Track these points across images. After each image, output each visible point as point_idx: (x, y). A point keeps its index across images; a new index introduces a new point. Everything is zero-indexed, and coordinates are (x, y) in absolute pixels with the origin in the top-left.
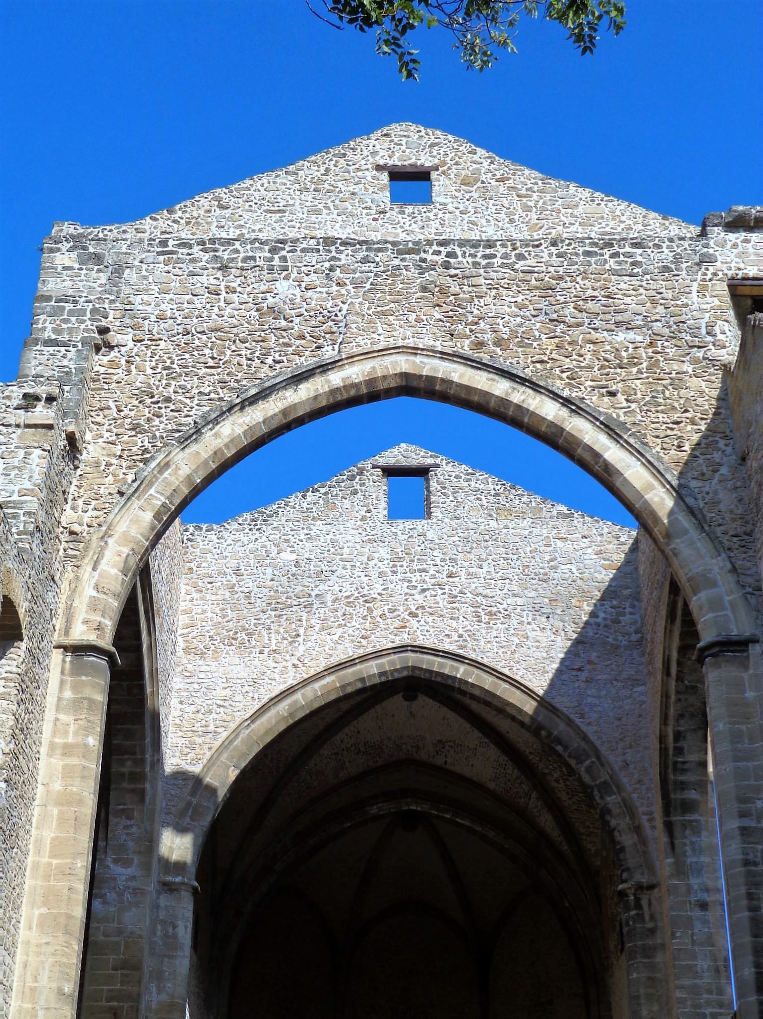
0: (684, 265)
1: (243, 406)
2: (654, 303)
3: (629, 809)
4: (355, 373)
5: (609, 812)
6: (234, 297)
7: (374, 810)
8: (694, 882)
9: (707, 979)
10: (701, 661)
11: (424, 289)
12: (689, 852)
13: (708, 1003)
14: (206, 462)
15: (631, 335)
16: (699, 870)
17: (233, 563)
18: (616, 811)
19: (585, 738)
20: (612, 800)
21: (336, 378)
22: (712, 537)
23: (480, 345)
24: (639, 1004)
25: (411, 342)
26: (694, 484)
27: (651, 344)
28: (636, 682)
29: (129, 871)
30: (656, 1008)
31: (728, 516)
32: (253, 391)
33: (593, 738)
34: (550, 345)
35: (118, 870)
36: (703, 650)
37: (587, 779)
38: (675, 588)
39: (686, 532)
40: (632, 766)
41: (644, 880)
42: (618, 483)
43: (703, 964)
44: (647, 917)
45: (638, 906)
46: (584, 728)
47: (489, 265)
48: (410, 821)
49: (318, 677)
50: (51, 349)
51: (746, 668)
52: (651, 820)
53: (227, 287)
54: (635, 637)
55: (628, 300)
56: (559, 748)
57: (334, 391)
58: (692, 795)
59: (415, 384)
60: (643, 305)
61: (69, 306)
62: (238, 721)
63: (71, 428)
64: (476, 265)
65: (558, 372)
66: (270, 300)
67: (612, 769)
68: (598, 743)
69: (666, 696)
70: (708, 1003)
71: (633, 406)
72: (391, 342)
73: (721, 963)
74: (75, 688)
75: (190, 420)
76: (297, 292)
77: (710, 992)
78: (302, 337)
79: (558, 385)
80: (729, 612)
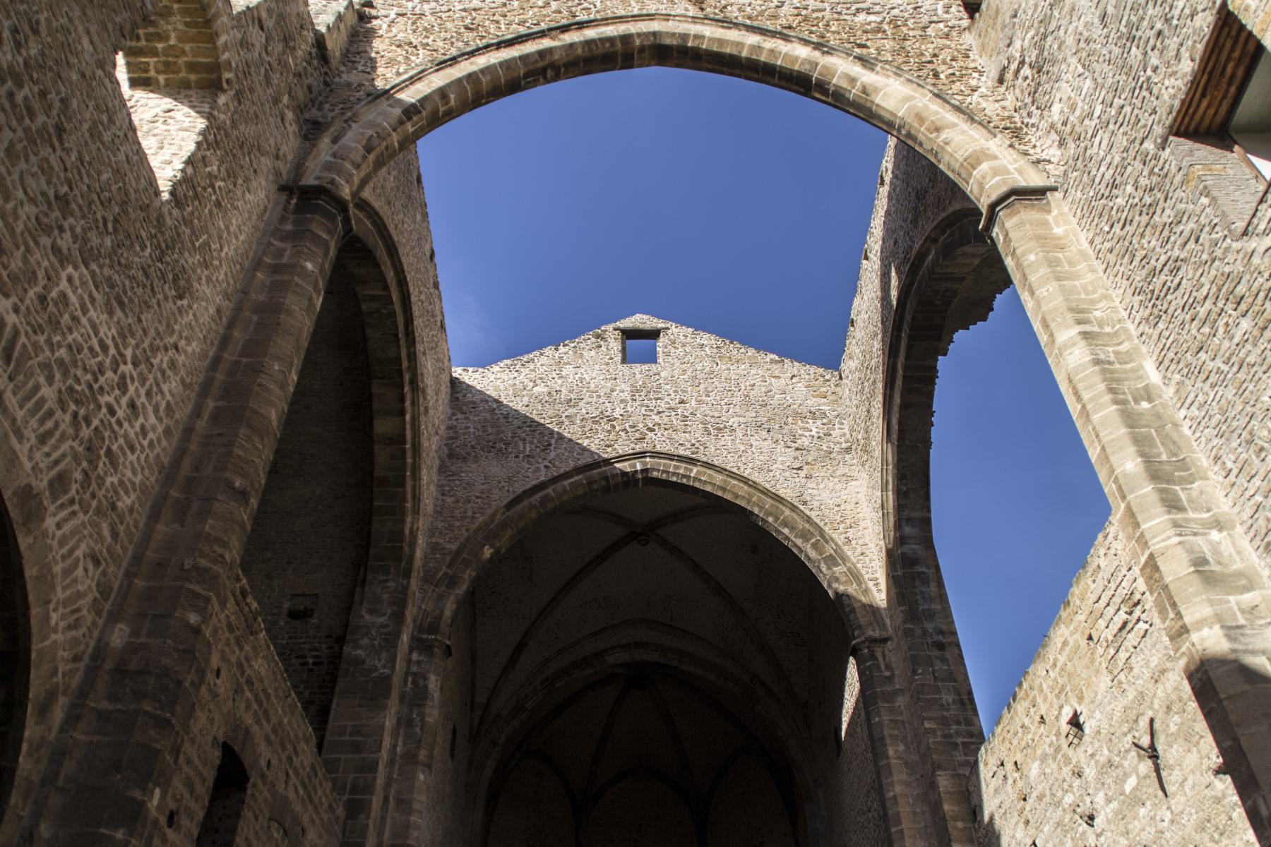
5: (837, 580)
8: (929, 626)
9: (953, 711)
12: (921, 601)
13: (958, 733)
15: (872, 18)
16: (931, 615)
19: (809, 520)
24: (885, 745)
31: (995, 118)
33: (817, 520)
39: (955, 125)
40: (853, 542)
41: (877, 634)
43: (947, 698)
44: (882, 666)
46: (808, 513)
51: (1049, 212)
54: (844, 445)
56: (786, 531)
67: (836, 544)
68: (821, 524)
70: (958, 733)
73: (965, 697)
74: (295, 223)
77: (959, 723)
80: (1016, 175)
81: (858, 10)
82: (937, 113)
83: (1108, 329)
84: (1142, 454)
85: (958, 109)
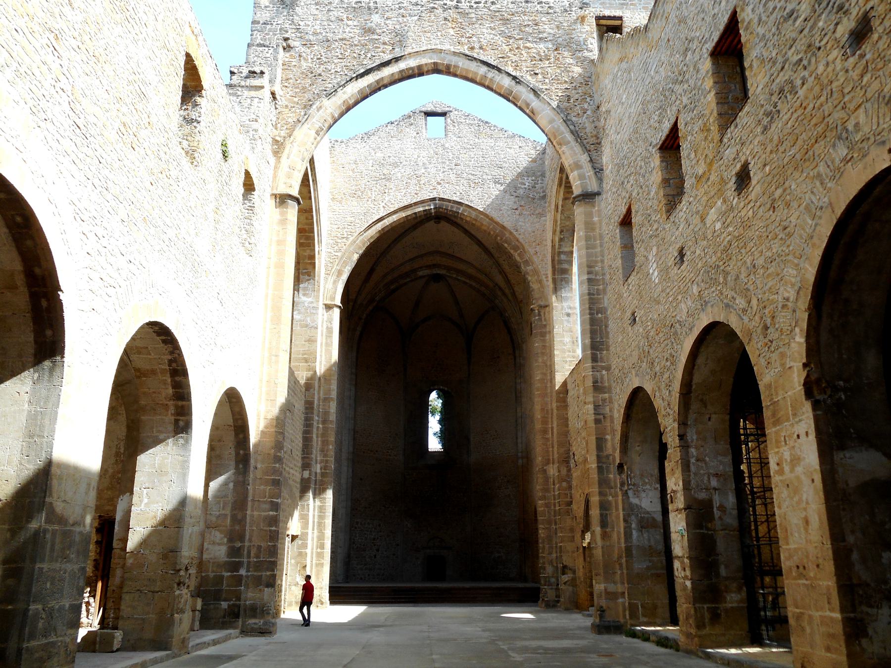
0: (574, 9)
1: (357, 78)
2: (558, 27)
3: (536, 272)
4: (412, 63)
5: (528, 273)
6: (350, 23)
7: (421, 273)
8: (565, 304)
9: (569, 346)
10: (573, 203)
11: (445, 19)
13: (568, 356)
14: (340, 107)
16: (567, 299)
17: (354, 158)
18: (531, 273)
20: (529, 268)
21: (402, 65)
22: (582, 145)
23: (472, 48)
25: (439, 47)
26: (574, 119)
27: (556, 50)
28: (541, 215)
29: (310, 299)
30: (545, 358)
31: (589, 135)
32: (362, 71)
33: (521, 240)
34: (507, 49)
35: (304, 299)
36: (574, 198)
37: (518, 259)
38: (562, 170)
39: (569, 142)
42: (538, 119)
45: (539, 315)
46: (517, 236)
47: (477, 8)
48: (437, 278)
49: (395, 212)
50: (261, 49)
51: (594, 206)
52: (547, 277)
53: (347, 17)
54: (542, 194)
55: (546, 27)
56: (506, 245)
57: (401, 72)
58: (565, 266)
59: (440, 68)
60: (552, 29)
61: (269, 27)
62: (358, 232)
63: (273, 89)
64: (471, 7)
65: (510, 63)
66: (369, 24)
69: (555, 221)
70: (568, 356)
71: (547, 80)
72: (429, 47)
74: (282, 214)
75: (330, 85)
76: (383, 20)
78: (384, 43)
79: (510, 70)
81: (540, 39)
82: (563, 133)
83: (598, 277)
84: (591, 338)
85: (572, 132)
